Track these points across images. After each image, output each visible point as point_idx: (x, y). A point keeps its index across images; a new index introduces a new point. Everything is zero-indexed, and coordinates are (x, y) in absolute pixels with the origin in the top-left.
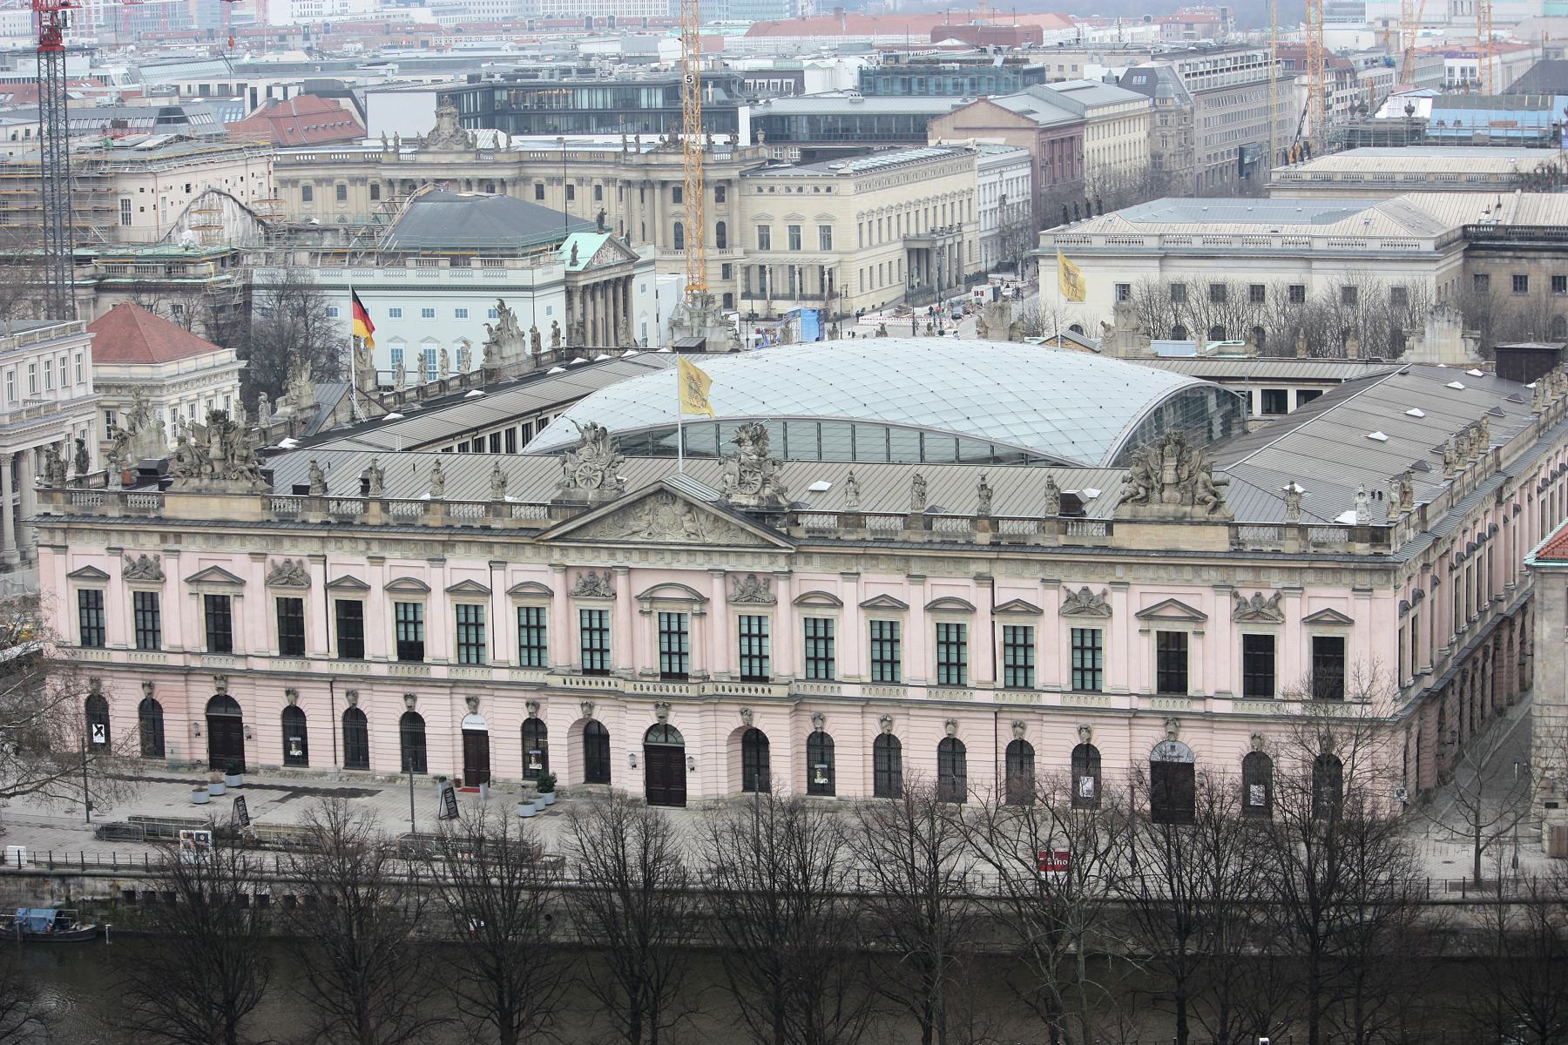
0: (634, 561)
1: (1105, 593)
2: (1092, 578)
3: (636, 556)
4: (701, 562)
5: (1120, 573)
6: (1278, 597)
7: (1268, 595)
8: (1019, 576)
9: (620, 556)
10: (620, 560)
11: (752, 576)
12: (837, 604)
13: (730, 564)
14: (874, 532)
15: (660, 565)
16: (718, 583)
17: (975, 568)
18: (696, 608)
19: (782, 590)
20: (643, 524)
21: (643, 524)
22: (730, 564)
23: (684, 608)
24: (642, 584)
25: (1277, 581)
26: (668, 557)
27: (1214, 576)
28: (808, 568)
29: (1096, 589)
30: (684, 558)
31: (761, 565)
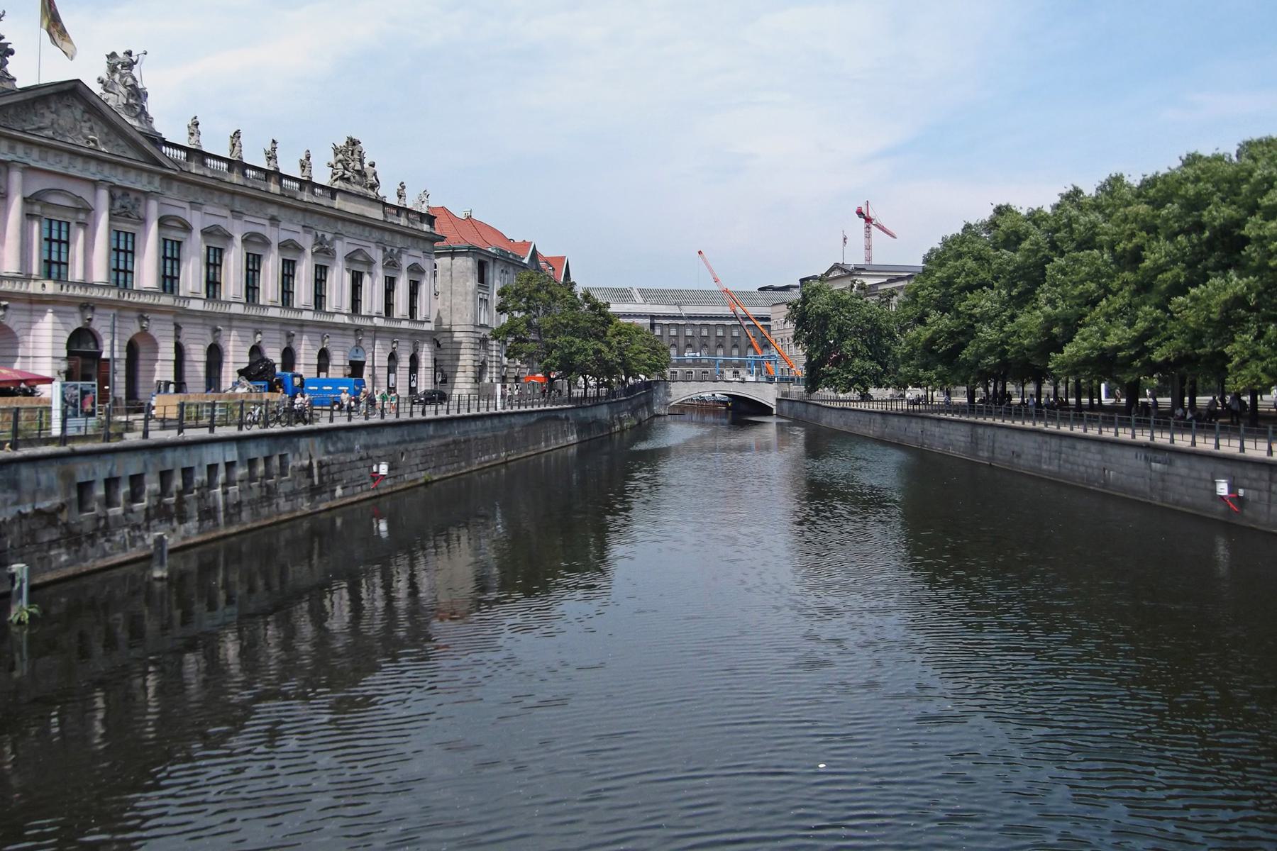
0: (34, 159)
1: (333, 240)
2: (328, 229)
3: (35, 153)
4: (92, 171)
5: (340, 225)
6: (400, 251)
7: (396, 251)
8: (291, 221)
9: (20, 149)
10: (20, 153)
11: (126, 191)
12: (187, 228)
13: (118, 178)
14: (213, 171)
15: (58, 168)
16: (103, 195)
17: (273, 211)
18: (82, 217)
19: (153, 210)
20: (47, 122)
21: (47, 122)
22: (118, 178)
23: (69, 216)
24: (38, 184)
25: (399, 242)
26: (66, 159)
27: (377, 234)
28: (168, 193)
29: (328, 237)
30: (79, 163)
31: (141, 183)
